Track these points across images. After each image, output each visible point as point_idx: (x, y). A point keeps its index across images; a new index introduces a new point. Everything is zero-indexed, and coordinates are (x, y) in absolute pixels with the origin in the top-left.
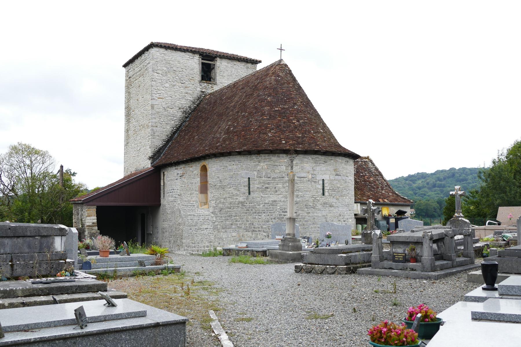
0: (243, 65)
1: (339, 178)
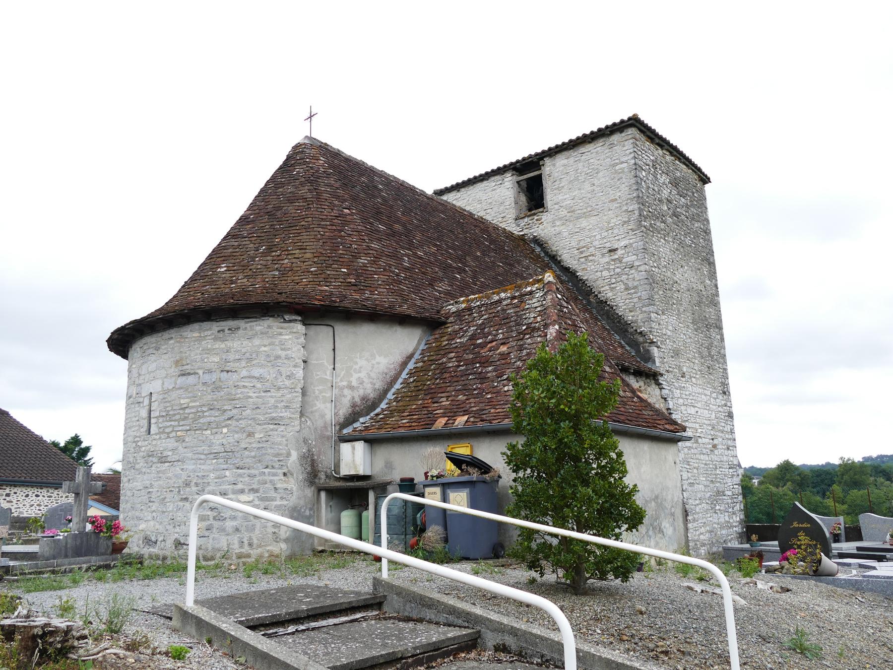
0: (601, 144)
1: (191, 380)
